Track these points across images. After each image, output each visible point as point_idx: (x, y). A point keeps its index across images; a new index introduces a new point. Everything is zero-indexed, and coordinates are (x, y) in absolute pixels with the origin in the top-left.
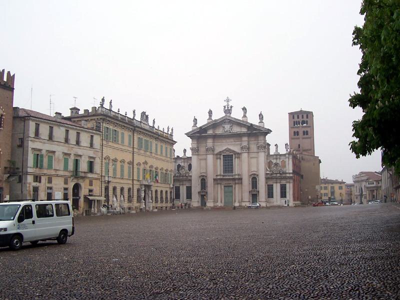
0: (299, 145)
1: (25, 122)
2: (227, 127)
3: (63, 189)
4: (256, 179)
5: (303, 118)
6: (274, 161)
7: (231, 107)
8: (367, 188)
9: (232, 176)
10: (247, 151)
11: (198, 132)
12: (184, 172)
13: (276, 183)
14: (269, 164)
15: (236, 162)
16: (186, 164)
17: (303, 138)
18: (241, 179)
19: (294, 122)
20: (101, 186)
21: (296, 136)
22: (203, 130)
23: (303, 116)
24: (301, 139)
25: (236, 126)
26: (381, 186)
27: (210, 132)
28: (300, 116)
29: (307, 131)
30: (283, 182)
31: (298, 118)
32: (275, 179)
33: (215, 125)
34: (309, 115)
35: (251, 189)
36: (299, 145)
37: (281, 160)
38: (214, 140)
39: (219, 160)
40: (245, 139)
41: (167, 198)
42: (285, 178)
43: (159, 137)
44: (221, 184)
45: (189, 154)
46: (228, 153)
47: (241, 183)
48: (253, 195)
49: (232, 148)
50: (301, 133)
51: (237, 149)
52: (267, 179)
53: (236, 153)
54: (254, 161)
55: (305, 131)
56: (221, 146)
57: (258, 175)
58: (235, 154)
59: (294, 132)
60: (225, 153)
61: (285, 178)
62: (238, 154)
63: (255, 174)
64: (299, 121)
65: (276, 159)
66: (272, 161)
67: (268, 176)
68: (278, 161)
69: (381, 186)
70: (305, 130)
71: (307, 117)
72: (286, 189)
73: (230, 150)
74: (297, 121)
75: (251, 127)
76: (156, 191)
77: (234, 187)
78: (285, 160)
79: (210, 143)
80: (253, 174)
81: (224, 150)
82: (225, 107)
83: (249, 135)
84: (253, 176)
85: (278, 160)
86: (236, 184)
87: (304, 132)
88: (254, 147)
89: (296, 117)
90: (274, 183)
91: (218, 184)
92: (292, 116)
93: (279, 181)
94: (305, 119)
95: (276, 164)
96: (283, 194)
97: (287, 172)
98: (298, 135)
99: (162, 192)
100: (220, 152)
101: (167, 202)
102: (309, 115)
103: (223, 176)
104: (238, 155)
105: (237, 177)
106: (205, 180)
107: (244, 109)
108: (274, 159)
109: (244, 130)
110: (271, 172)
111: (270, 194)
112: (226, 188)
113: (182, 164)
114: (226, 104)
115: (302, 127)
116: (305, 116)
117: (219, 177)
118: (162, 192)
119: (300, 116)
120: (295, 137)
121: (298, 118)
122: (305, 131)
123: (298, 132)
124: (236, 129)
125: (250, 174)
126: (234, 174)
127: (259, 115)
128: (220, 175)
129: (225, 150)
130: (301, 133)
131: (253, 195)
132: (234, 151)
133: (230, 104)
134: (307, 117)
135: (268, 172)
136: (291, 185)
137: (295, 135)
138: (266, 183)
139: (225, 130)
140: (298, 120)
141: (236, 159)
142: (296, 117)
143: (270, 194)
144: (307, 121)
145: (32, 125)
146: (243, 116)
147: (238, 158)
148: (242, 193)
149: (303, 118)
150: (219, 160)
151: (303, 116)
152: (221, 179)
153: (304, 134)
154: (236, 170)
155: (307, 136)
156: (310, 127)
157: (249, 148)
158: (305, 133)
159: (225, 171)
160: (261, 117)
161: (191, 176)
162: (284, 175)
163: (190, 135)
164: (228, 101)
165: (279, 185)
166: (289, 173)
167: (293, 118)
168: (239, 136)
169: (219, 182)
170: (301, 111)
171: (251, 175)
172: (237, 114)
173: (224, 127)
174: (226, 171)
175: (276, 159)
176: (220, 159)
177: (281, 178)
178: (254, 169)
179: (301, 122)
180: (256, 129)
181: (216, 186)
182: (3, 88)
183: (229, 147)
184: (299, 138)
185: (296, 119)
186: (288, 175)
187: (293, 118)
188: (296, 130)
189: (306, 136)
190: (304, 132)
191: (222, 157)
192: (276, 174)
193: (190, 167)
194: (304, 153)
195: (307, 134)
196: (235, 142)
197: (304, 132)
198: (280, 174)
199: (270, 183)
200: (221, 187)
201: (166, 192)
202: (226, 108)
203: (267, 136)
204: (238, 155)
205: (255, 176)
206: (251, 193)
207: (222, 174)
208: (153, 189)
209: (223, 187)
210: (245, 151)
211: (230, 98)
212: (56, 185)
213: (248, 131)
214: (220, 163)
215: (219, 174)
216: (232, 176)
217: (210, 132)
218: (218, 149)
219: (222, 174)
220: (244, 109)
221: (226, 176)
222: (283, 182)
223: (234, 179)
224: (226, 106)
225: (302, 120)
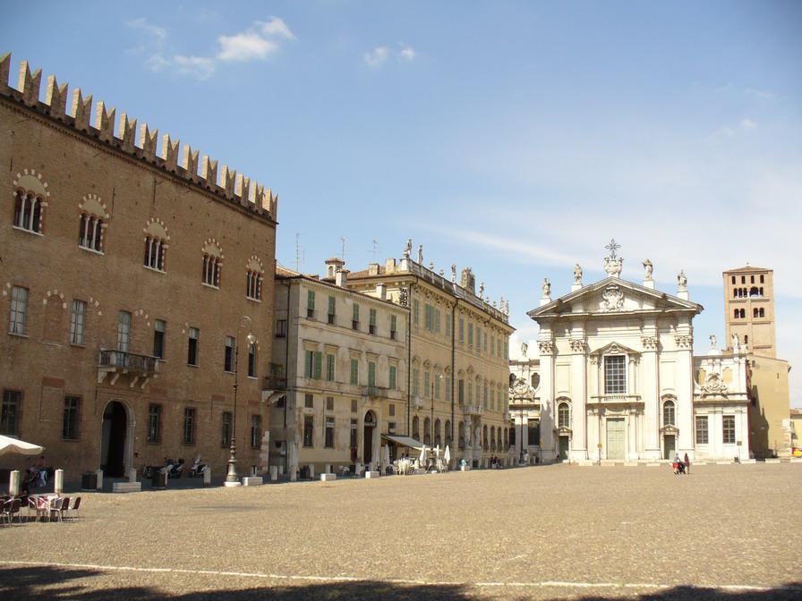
0: (746, 337)
1: (289, 287)
3: (350, 422)
4: (673, 405)
5: (753, 281)
11: (555, 311)
12: (525, 390)
15: (629, 368)
16: (526, 373)
19: (735, 290)
20: (407, 417)
21: (740, 320)
22: (563, 306)
23: (752, 278)
24: (750, 325)
27: (578, 311)
28: (748, 278)
31: (743, 281)
33: (590, 296)
34: (763, 274)
36: (746, 337)
37: (723, 367)
38: (586, 329)
41: (500, 441)
42: (735, 404)
43: (493, 321)
45: (534, 353)
50: (749, 313)
51: (636, 345)
52: (696, 405)
56: (602, 339)
58: (630, 355)
59: (736, 311)
61: (735, 404)
63: (671, 396)
64: (745, 289)
67: (698, 399)
68: (717, 369)
70: (758, 305)
71: (762, 281)
72: (733, 426)
74: (740, 289)
75: (663, 301)
76: (485, 427)
78: (731, 367)
79: (577, 333)
80: (666, 396)
89: (739, 279)
91: (595, 414)
92: (731, 277)
93: (719, 409)
94: (758, 284)
95: (715, 377)
96: (729, 436)
98: (743, 316)
99: (493, 428)
101: (493, 449)
102: (766, 277)
104: (636, 356)
105: (634, 400)
106: (566, 405)
109: (648, 307)
111: (701, 436)
112: (611, 424)
113: (519, 375)
115: (753, 301)
116: (757, 278)
117: (596, 401)
118: (493, 428)
119: (748, 278)
121: (743, 281)
123: (743, 311)
124: (631, 306)
129: (609, 346)
130: (749, 313)
131: (666, 437)
132: (628, 350)
134: (762, 281)
136: (745, 417)
137: (736, 316)
138: (694, 413)
139: (610, 306)
140: (743, 286)
142: (739, 279)
143: (701, 436)
144: (762, 289)
145: (303, 292)
149: (753, 281)
151: (752, 278)
154: (630, 388)
155: (762, 319)
156: (768, 300)
158: (759, 312)
159: (608, 389)
160: (682, 280)
161: (539, 399)
162: (731, 398)
163: (541, 318)
164: (613, 247)
166: (741, 394)
167: (734, 282)
170: (748, 268)
172: (632, 274)
173: (607, 301)
174: (610, 388)
176: (599, 364)
178: (667, 386)
179: (749, 290)
180: (672, 305)
182: (261, 222)
184: (745, 324)
185: (739, 285)
186: (738, 398)
187: (734, 282)
188: (739, 306)
189: (759, 319)
190: (756, 311)
192: (714, 395)
193: (536, 379)
194: (756, 352)
198: (723, 395)
201: (500, 429)
203: (693, 319)
204: (636, 356)
206: (662, 434)
207: (602, 394)
208: (483, 422)
209: (604, 419)
210: (650, 349)
211: (617, 242)
212: (339, 412)
213: (657, 307)
214: (597, 373)
217: (578, 311)
218: (595, 343)
219: (602, 394)
222: (729, 411)
223: (628, 406)
224: (610, 259)
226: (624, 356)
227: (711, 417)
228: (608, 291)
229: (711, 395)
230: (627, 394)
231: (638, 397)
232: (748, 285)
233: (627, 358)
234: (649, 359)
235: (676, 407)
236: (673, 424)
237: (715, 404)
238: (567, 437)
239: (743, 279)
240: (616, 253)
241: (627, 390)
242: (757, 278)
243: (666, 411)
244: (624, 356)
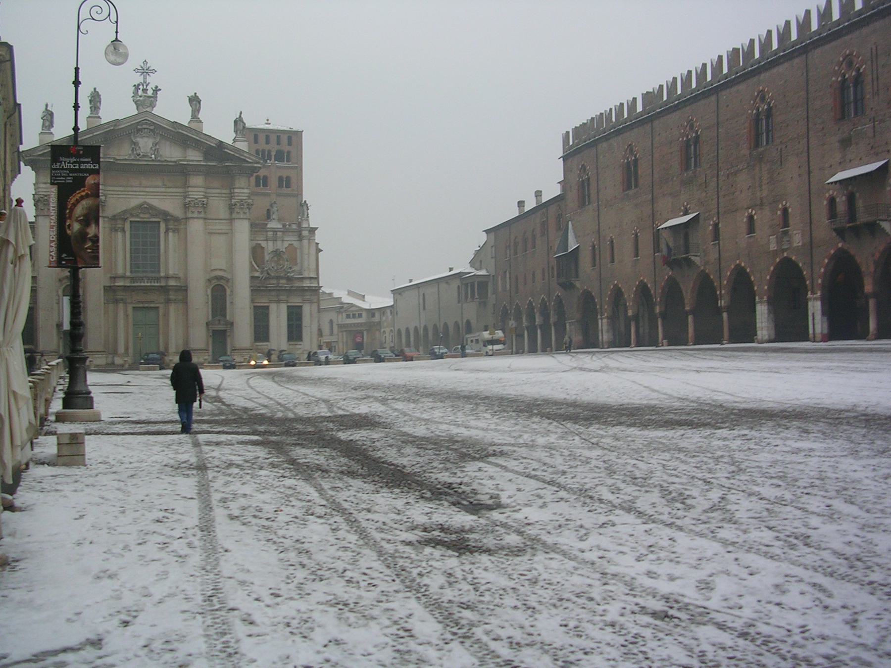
2: (145, 144)
4: (225, 290)
5: (278, 143)
6: (270, 246)
7: (156, 90)
8: (340, 326)
9: (158, 279)
10: (202, 215)
13: (279, 302)
14: (256, 252)
15: (170, 243)
17: (279, 195)
18: (184, 289)
25: (168, 143)
26: (379, 323)
29: (288, 179)
30: (296, 301)
31: (268, 142)
32: (273, 293)
35: (210, 318)
37: (286, 244)
39: (120, 235)
40: (197, 181)
44: (125, 303)
46: (145, 217)
47: (185, 301)
48: (214, 332)
49: (156, 202)
50: (273, 182)
51: (170, 205)
53: (166, 216)
54: (219, 242)
55: (285, 176)
57: (228, 280)
58: (166, 221)
60: (137, 216)
62: (177, 220)
63: (222, 278)
64: (269, 152)
65: (275, 240)
66: (263, 244)
68: (282, 246)
69: (379, 323)
70: (285, 174)
71: (290, 144)
73: (151, 207)
74: (263, 151)
77: (161, 311)
81: (133, 209)
82: (137, 87)
83: (208, 173)
84: (215, 282)
85: (279, 243)
86: (168, 301)
87: (280, 179)
88: (218, 206)
90: (271, 301)
91: (116, 302)
93: (283, 298)
94: (285, 148)
95: (277, 253)
97: (306, 275)
100: (125, 212)
102: (294, 138)
103: (133, 279)
104: (175, 223)
105: (172, 283)
107: (195, 101)
108: (267, 240)
109: (194, 156)
110: (265, 275)
114: (139, 79)
117: (120, 283)
120: (258, 190)
121: (268, 142)
122: (285, 176)
124: (171, 153)
125: (208, 278)
126: (162, 274)
127: (236, 122)
128: (124, 277)
130: (273, 182)
133: (153, 81)
134: (290, 144)
135: (257, 274)
138: (252, 301)
140: (267, 147)
141: (171, 234)
144: (289, 152)
146: (189, 118)
147: (174, 231)
148: (187, 327)
149: (278, 143)
150: (120, 235)
152: (125, 288)
153: (280, 185)
154: (171, 265)
157: (205, 206)
159: (134, 267)
165: (284, 308)
167: (256, 141)
168: (182, 171)
169: (120, 295)
171: (209, 280)
173: (135, 144)
175: (275, 240)
176: (123, 230)
177: (290, 292)
178: (219, 263)
179: (273, 154)
180: (231, 158)
181: (111, 307)
183: (149, 201)
185: (262, 145)
187: (256, 141)
189: (285, 190)
191: (127, 226)
195: (288, 186)
196: (165, 186)
197: (280, 179)
199: (262, 301)
200: (126, 312)
202: (140, 92)
205: (222, 282)
207: (128, 274)
210: (196, 215)
213: (206, 158)
215: (120, 271)
216: (158, 279)
219: (128, 274)
220: (195, 101)
221: (141, 279)
223: (165, 290)
224: (141, 87)
225: (277, 147)
226: (159, 222)
227: (273, 307)
228: (139, 130)
229: (273, 278)
230: (162, 274)
231: (177, 278)
232: (273, 147)
233: (163, 226)
234: (196, 227)
235: (228, 292)
236: (225, 316)
237: (279, 290)
238: (224, 331)
239: (268, 137)
240: (149, 79)
241: (162, 269)
242: (284, 139)
243: (214, 298)
244: (159, 222)
